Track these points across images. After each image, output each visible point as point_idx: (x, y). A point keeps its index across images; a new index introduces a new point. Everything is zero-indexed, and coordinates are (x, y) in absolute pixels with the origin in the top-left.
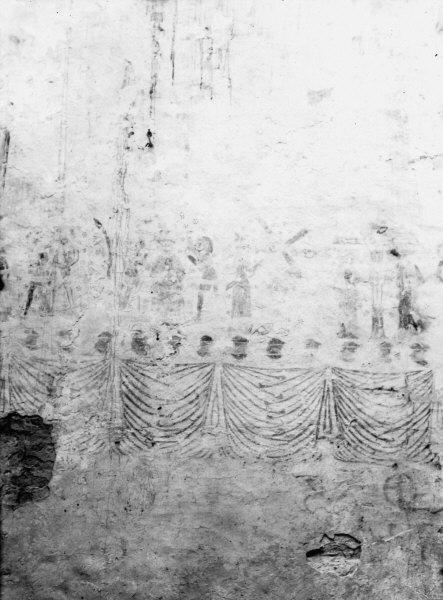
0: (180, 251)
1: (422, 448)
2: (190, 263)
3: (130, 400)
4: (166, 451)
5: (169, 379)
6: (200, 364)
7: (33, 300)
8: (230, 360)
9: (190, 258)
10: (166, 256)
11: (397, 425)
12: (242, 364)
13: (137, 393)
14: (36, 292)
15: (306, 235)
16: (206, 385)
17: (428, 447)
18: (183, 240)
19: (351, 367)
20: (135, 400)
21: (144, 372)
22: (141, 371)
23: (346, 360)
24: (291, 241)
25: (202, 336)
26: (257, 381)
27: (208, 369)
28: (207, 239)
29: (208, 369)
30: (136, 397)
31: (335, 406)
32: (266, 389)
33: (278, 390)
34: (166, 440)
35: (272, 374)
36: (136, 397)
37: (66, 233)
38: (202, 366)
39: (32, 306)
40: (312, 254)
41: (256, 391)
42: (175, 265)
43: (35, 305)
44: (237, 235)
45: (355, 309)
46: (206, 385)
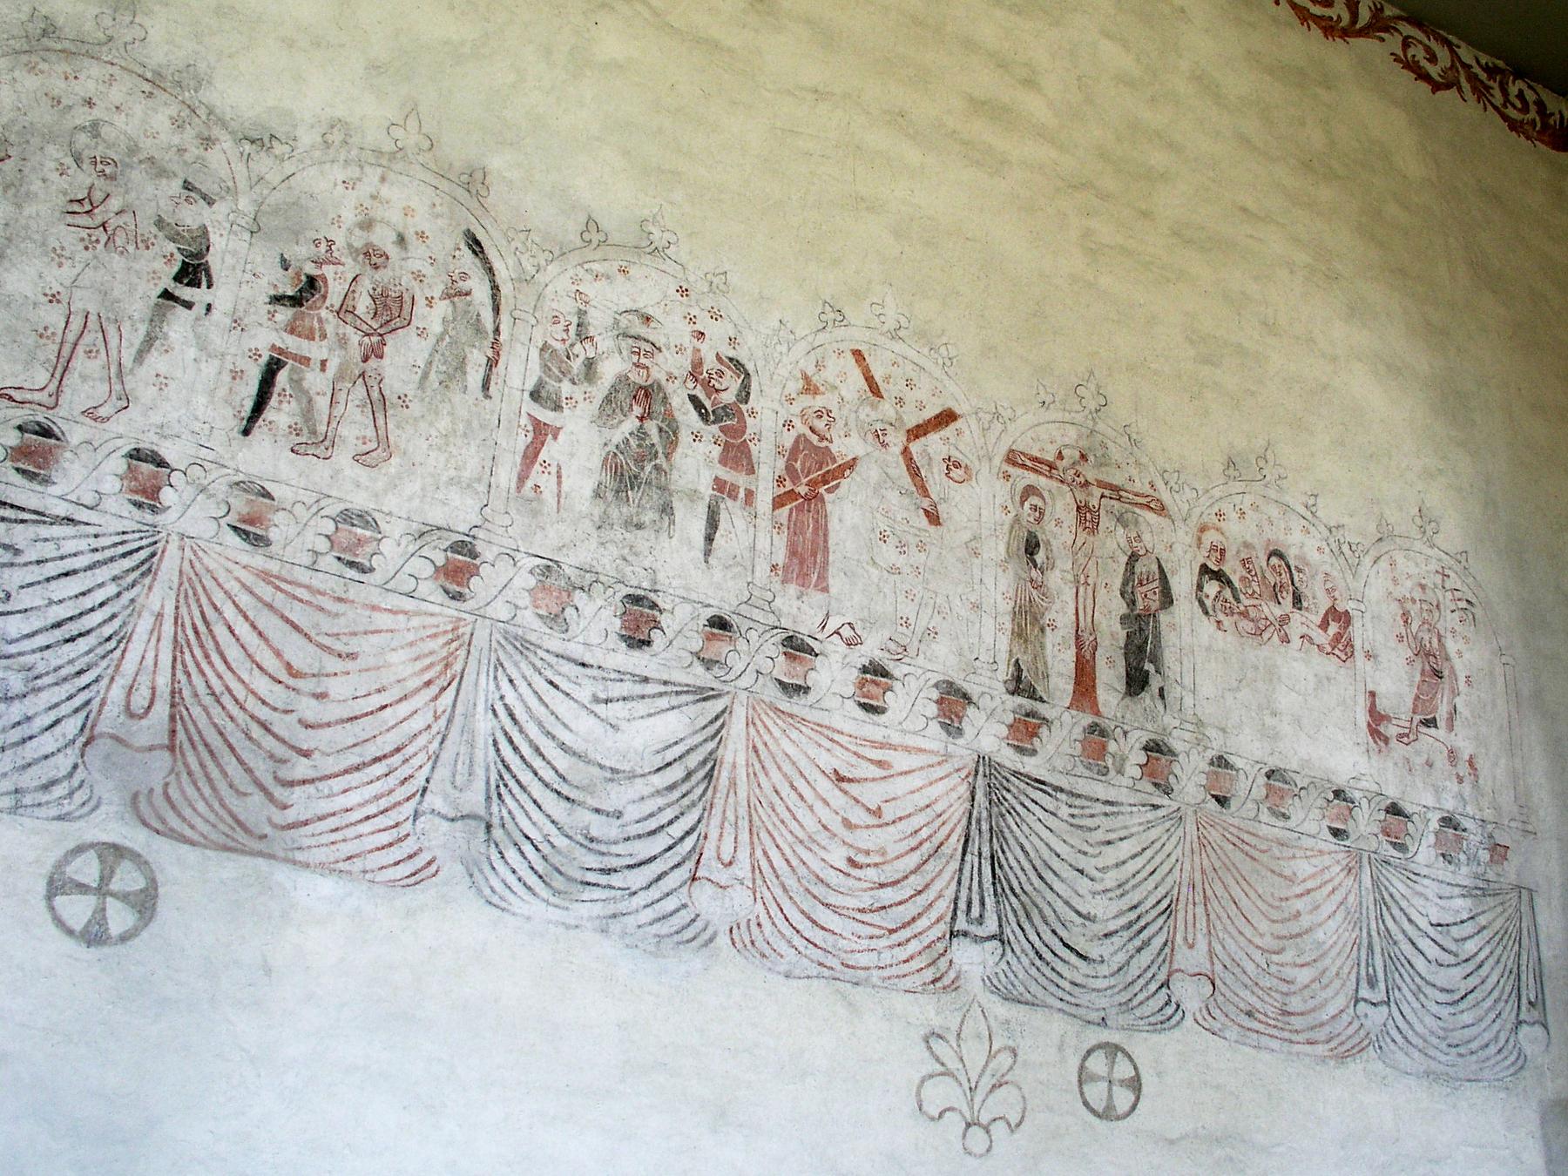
0: (671, 377)
1: (1153, 987)
2: (694, 414)
3: (516, 749)
4: (598, 909)
5: (616, 711)
6: (701, 689)
7: (274, 401)
8: (772, 693)
9: (694, 399)
10: (638, 378)
11: (1112, 926)
12: (795, 710)
13: (533, 730)
14: (282, 378)
15: (953, 426)
16: (711, 745)
17: (1166, 984)
18: (680, 350)
19: (1030, 766)
20: (526, 750)
21: (557, 680)
22: (549, 674)
23: (1020, 750)
24: (918, 432)
25: (710, 612)
26: (828, 761)
27: (719, 705)
28: (737, 365)
29: (719, 705)
30: (531, 742)
31: (992, 857)
32: (844, 785)
33: (872, 794)
34: (603, 879)
35: (860, 750)
36: (531, 742)
37: (383, 238)
38: (704, 695)
39: (269, 414)
40: (960, 472)
41: (825, 786)
42: (658, 408)
43: (280, 414)
44: (806, 378)
45: (1042, 630)
46: (711, 745)
